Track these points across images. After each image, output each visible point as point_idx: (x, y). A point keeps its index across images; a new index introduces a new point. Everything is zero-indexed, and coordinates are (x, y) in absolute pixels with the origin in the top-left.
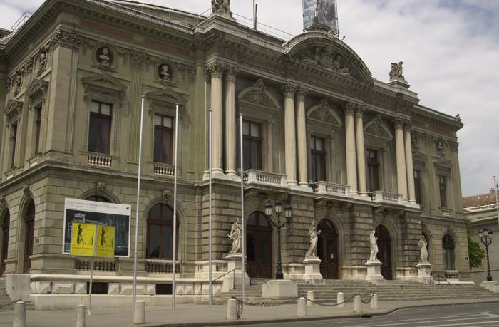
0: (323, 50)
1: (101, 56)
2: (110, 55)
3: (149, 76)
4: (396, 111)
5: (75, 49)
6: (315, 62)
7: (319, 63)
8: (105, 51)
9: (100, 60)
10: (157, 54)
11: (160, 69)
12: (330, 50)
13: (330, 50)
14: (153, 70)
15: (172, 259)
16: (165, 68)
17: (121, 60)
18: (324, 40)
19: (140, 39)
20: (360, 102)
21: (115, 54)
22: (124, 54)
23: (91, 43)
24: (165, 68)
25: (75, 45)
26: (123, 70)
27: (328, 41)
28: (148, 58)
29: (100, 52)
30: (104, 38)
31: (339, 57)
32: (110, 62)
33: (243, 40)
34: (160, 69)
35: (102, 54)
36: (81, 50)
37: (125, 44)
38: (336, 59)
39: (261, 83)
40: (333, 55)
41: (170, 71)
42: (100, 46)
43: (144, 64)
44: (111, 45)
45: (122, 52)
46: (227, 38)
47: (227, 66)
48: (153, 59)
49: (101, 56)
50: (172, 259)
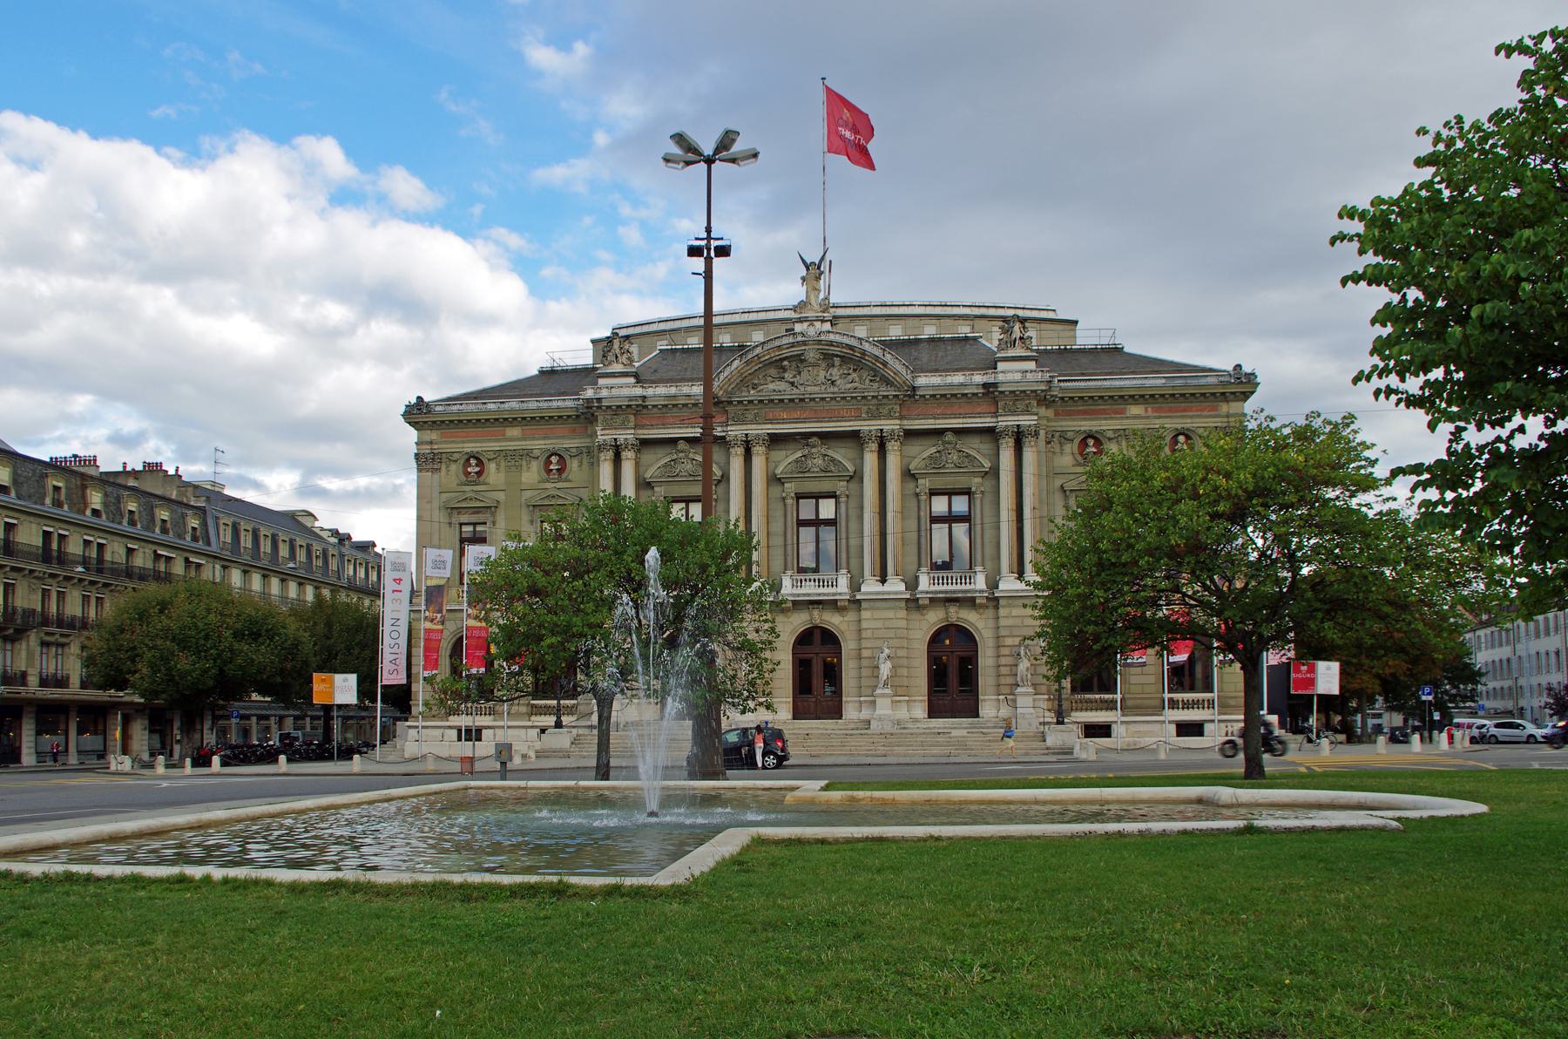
0: (799, 359)
1: (469, 470)
2: (480, 463)
3: (531, 474)
4: (995, 414)
5: (435, 470)
6: (782, 386)
7: (792, 384)
9: (467, 474)
10: (539, 445)
12: (811, 355)
15: (1212, 691)
16: (554, 459)
18: (793, 345)
19: (514, 432)
20: (890, 425)
21: (485, 461)
23: (456, 456)
24: (554, 459)
25: (435, 466)
26: (495, 474)
27: (804, 343)
28: (528, 455)
30: (470, 447)
32: (479, 474)
33: (631, 398)
34: (548, 462)
35: (470, 465)
36: (444, 467)
37: (496, 446)
38: (833, 366)
42: (466, 457)
43: (524, 463)
44: (478, 452)
46: (605, 403)
48: (536, 453)
49: (469, 470)
50: (1212, 691)
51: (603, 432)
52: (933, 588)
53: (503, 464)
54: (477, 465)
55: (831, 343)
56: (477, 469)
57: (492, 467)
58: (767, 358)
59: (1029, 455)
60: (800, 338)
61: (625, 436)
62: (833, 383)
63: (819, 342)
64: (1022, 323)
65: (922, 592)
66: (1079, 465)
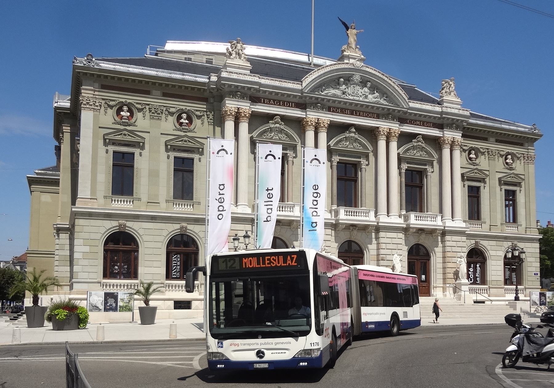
1: (122, 113)
2: (130, 110)
7: (344, 93)
8: (125, 108)
11: (179, 117)
12: (357, 77)
13: (357, 77)
14: (172, 119)
16: (184, 116)
17: (140, 115)
22: (143, 109)
23: (112, 103)
24: (184, 116)
29: (120, 110)
31: (369, 84)
34: (179, 117)
38: (366, 86)
39: (278, 119)
40: (361, 82)
41: (189, 118)
45: (141, 107)
47: (238, 108)
48: (172, 110)
53: (147, 113)
54: (128, 111)
62: (366, 97)
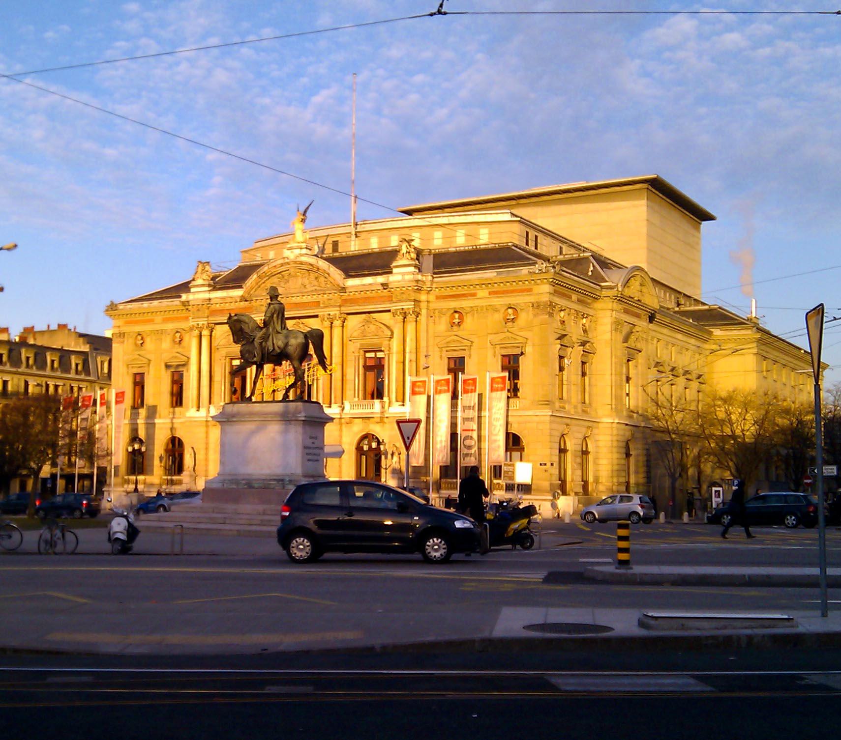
3: (166, 344)
10: (170, 326)
18: (282, 265)
23: (131, 334)
26: (149, 344)
27: (288, 263)
51: (193, 320)
52: (352, 411)
55: (302, 263)
56: (141, 342)
57: (148, 340)
58: (270, 273)
59: (410, 328)
60: (287, 261)
61: (202, 323)
63: (295, 262)
64: (408, 243)
65: (346, 414)
66: (449, 331)
